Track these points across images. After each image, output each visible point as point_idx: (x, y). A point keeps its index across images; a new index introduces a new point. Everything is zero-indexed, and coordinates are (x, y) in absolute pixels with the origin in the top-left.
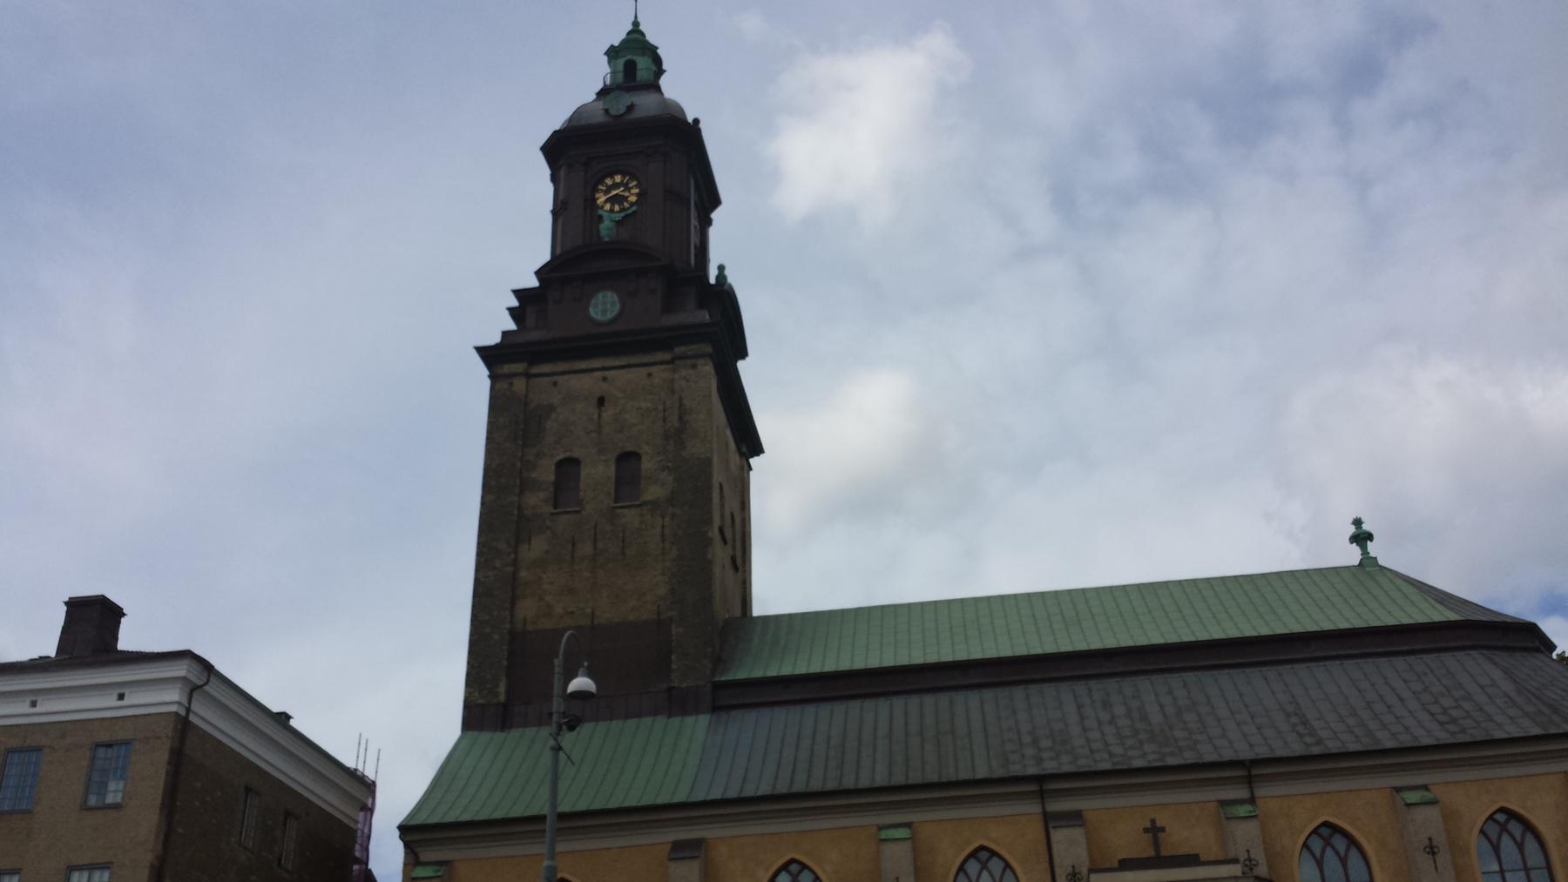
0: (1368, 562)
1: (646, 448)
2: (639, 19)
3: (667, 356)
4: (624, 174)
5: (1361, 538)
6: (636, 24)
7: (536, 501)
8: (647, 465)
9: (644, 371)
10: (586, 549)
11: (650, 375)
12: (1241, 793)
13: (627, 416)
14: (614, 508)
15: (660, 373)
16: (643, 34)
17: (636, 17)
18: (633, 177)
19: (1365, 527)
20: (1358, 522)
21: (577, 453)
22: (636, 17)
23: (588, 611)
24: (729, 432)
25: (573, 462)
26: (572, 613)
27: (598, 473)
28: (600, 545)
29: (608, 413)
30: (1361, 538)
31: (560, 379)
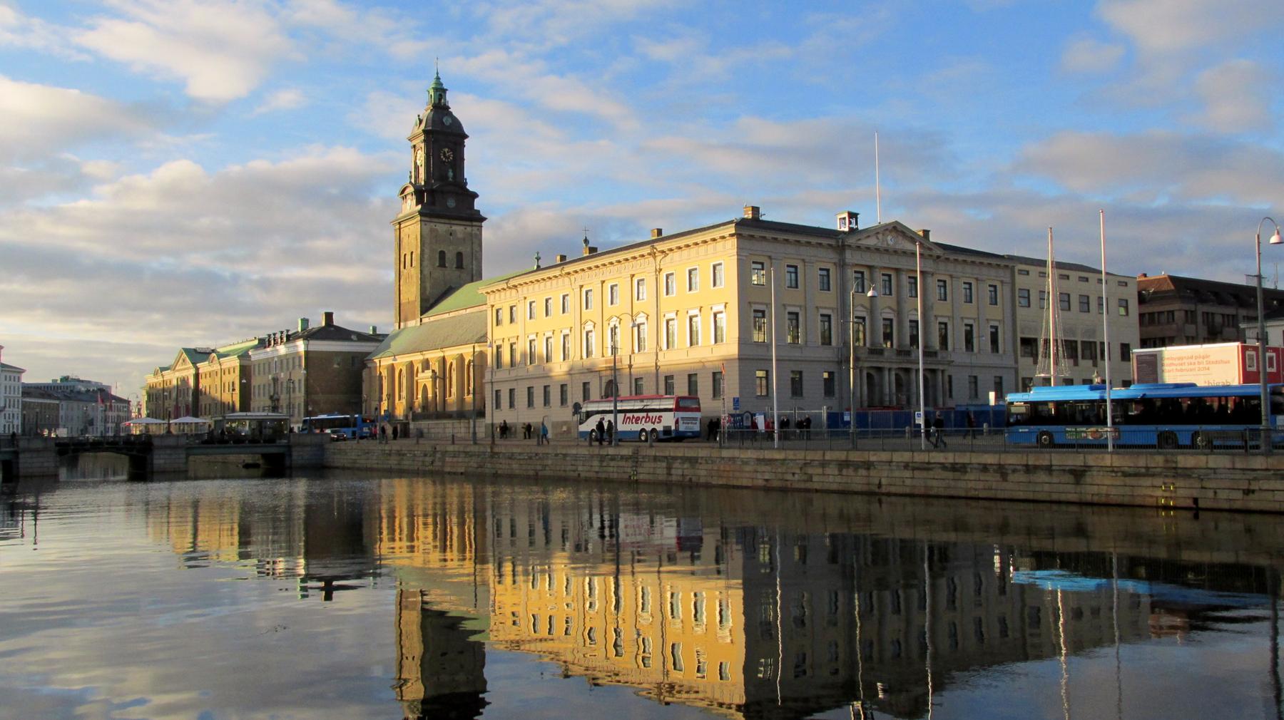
6: (437, 74)
24: (454, 228)
27: (408, 258)
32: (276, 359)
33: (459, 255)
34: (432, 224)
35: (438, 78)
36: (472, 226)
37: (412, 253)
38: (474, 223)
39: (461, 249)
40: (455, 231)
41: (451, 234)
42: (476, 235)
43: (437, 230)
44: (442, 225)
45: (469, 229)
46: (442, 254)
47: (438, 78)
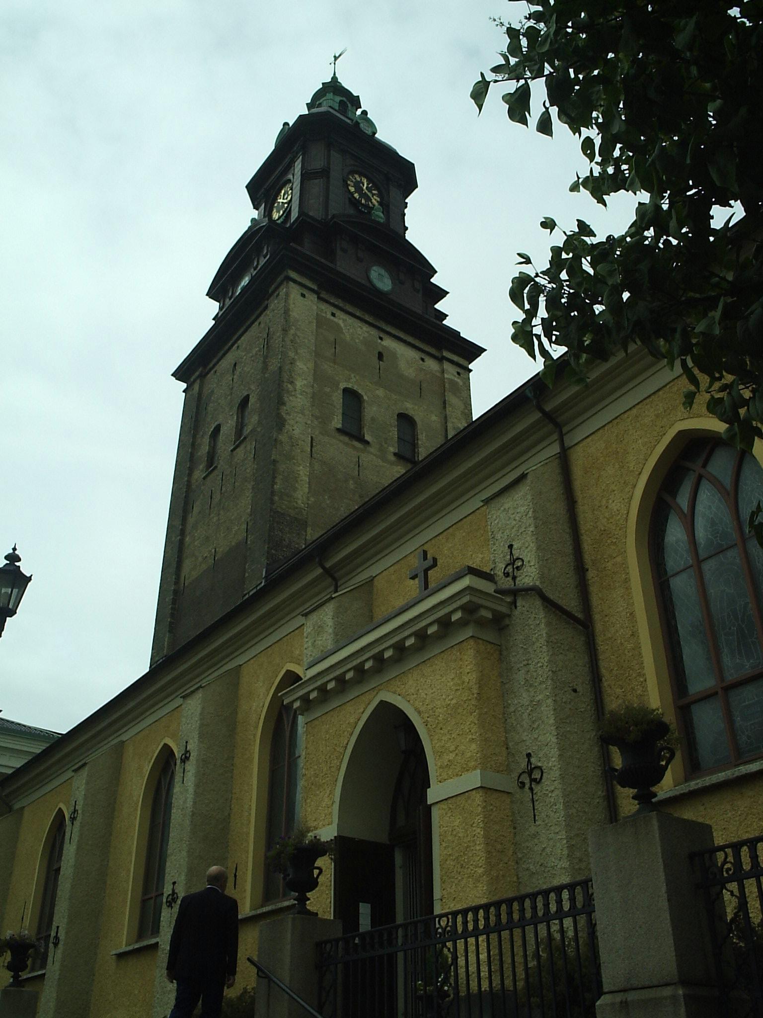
1: (253, 387)
2: (337, 75)
7: (199, 474)
8: (252, 400)
9: (257, 323)
10: (217, 497)
11: (260, 323)
13: (245, 369)
14: (232, 451)
17: (335, 74)
22: (335, 74)
23: (213, 550)
25: (218, 429)
26: (206, 557)
27: (229, 426)
28: (224, 489)
31: (217, 368)
33: (405, 420)
34: (324, 306)
35: (334, 78)
36: (441, 360)
37: (245, 401)
38: (446, 354)
39: (410, 407)
40: (394, 355)
41: (380, 356)
42: (452, 382)
43: (339, 329)
44: (357, 323)
45: (432, 365)
46: (352, 397)
47: (334, 78)
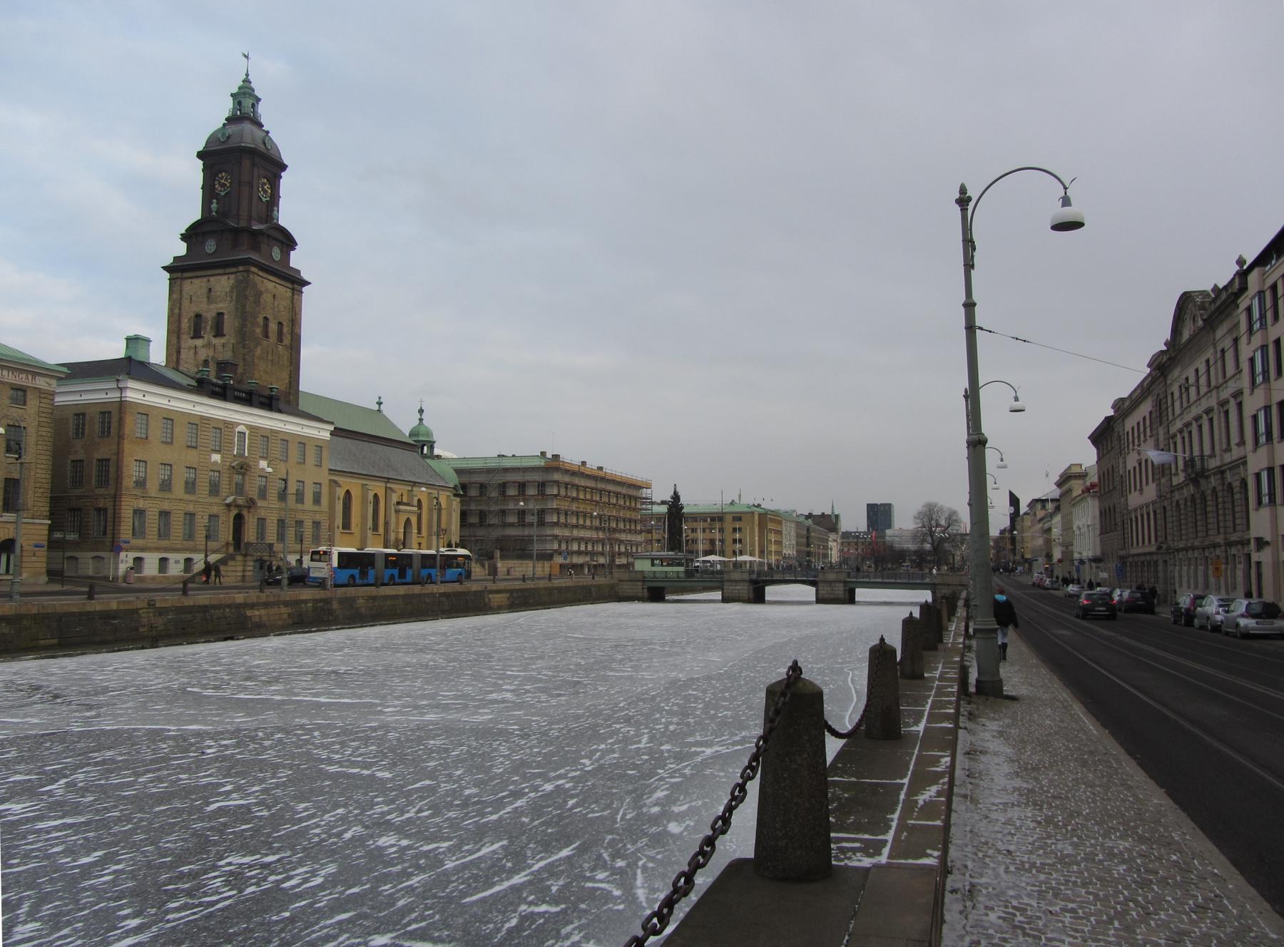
0: (379, 411)
1: (284, 323)
3: (290, 286)
4: (268, 180)
5: (380, 404)
6: (247, 75)
10: (270, 357)
12: (410, 488)
15: (289, 294)
16: (250, 82)
18: (270, 184)
19: (382, 400)
20: (380, 398)
21: (268, 317)
27: (273, 327)
29: (276, 303)
30: (380, 404)
31: (265, 281)
32: (241, 428)
